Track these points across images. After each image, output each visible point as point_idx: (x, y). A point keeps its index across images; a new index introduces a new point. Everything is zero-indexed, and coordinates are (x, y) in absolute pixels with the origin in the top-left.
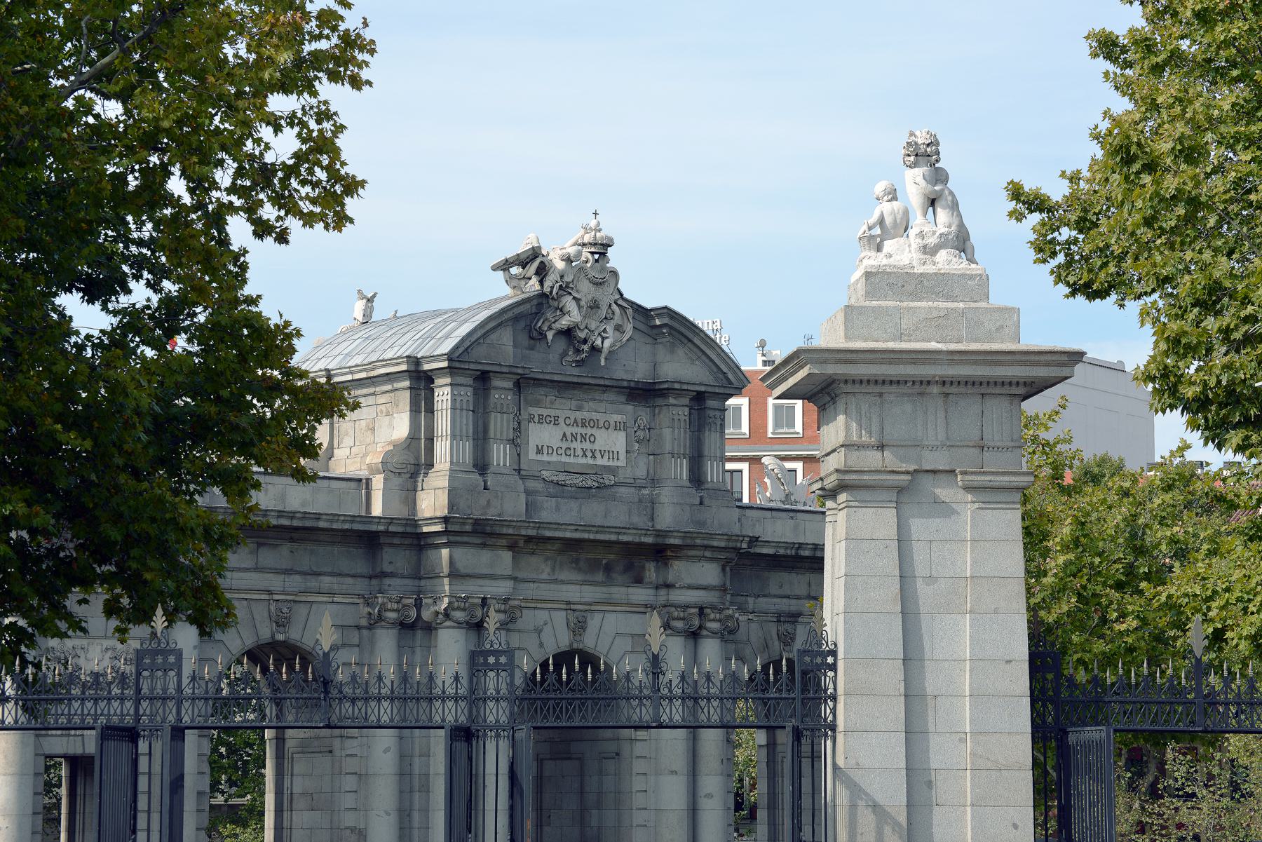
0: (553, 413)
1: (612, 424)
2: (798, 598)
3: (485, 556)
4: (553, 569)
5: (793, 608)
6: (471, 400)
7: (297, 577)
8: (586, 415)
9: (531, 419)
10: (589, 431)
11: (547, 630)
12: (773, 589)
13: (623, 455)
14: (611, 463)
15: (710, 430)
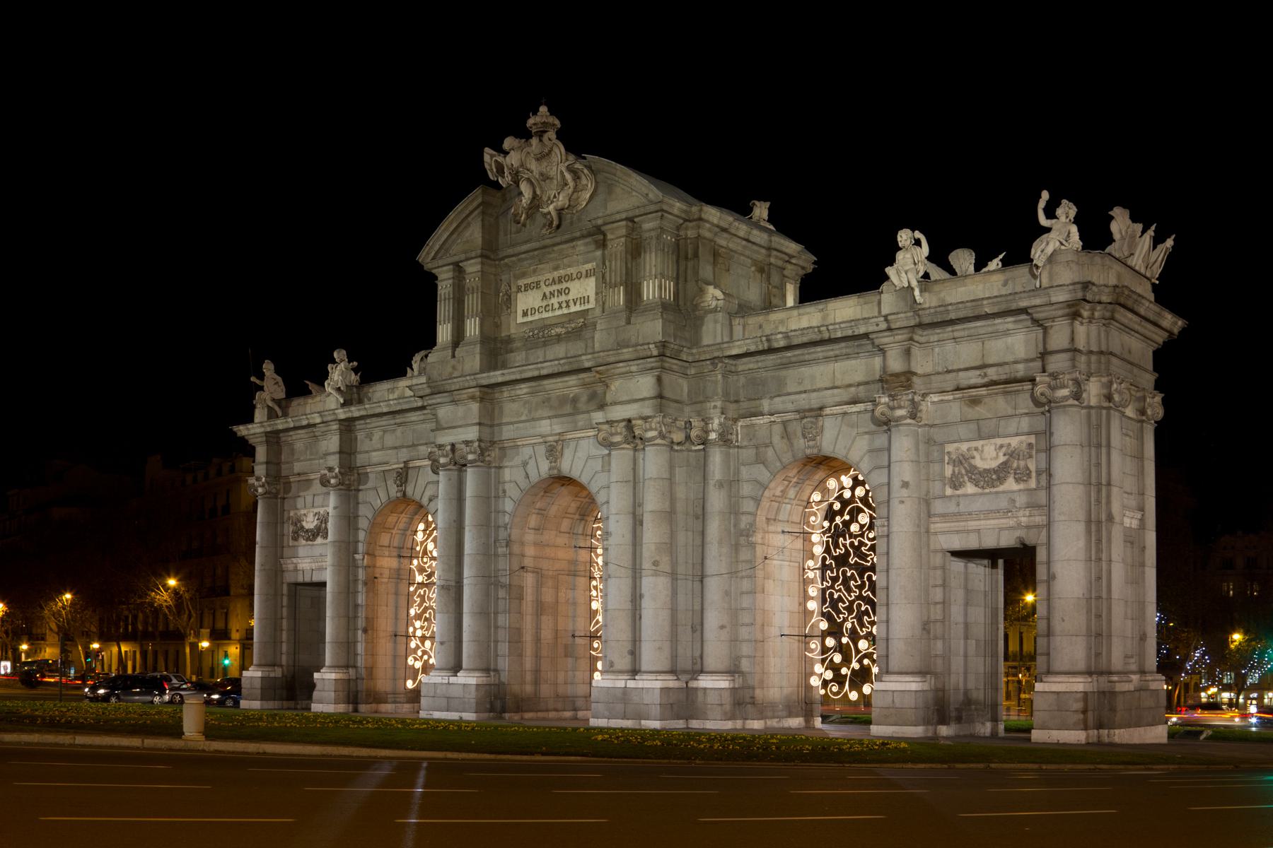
0: (534, 279)
1: (584, 273)
2: (814, 391)
3: (460, 410)
4: (530, 412)
5: (815, 404)
6: (451, 289)
7: (404, 450)
8: (562, 272)
9: (519, 290)
10: (564, 285)
11: (532, 463)
12: (792, 387)
13: (592, 299)
14: (583, 308)
15: (645, 252)
